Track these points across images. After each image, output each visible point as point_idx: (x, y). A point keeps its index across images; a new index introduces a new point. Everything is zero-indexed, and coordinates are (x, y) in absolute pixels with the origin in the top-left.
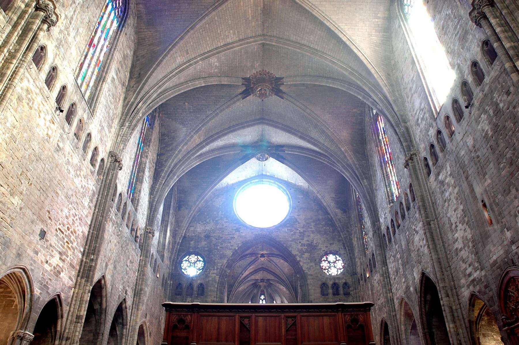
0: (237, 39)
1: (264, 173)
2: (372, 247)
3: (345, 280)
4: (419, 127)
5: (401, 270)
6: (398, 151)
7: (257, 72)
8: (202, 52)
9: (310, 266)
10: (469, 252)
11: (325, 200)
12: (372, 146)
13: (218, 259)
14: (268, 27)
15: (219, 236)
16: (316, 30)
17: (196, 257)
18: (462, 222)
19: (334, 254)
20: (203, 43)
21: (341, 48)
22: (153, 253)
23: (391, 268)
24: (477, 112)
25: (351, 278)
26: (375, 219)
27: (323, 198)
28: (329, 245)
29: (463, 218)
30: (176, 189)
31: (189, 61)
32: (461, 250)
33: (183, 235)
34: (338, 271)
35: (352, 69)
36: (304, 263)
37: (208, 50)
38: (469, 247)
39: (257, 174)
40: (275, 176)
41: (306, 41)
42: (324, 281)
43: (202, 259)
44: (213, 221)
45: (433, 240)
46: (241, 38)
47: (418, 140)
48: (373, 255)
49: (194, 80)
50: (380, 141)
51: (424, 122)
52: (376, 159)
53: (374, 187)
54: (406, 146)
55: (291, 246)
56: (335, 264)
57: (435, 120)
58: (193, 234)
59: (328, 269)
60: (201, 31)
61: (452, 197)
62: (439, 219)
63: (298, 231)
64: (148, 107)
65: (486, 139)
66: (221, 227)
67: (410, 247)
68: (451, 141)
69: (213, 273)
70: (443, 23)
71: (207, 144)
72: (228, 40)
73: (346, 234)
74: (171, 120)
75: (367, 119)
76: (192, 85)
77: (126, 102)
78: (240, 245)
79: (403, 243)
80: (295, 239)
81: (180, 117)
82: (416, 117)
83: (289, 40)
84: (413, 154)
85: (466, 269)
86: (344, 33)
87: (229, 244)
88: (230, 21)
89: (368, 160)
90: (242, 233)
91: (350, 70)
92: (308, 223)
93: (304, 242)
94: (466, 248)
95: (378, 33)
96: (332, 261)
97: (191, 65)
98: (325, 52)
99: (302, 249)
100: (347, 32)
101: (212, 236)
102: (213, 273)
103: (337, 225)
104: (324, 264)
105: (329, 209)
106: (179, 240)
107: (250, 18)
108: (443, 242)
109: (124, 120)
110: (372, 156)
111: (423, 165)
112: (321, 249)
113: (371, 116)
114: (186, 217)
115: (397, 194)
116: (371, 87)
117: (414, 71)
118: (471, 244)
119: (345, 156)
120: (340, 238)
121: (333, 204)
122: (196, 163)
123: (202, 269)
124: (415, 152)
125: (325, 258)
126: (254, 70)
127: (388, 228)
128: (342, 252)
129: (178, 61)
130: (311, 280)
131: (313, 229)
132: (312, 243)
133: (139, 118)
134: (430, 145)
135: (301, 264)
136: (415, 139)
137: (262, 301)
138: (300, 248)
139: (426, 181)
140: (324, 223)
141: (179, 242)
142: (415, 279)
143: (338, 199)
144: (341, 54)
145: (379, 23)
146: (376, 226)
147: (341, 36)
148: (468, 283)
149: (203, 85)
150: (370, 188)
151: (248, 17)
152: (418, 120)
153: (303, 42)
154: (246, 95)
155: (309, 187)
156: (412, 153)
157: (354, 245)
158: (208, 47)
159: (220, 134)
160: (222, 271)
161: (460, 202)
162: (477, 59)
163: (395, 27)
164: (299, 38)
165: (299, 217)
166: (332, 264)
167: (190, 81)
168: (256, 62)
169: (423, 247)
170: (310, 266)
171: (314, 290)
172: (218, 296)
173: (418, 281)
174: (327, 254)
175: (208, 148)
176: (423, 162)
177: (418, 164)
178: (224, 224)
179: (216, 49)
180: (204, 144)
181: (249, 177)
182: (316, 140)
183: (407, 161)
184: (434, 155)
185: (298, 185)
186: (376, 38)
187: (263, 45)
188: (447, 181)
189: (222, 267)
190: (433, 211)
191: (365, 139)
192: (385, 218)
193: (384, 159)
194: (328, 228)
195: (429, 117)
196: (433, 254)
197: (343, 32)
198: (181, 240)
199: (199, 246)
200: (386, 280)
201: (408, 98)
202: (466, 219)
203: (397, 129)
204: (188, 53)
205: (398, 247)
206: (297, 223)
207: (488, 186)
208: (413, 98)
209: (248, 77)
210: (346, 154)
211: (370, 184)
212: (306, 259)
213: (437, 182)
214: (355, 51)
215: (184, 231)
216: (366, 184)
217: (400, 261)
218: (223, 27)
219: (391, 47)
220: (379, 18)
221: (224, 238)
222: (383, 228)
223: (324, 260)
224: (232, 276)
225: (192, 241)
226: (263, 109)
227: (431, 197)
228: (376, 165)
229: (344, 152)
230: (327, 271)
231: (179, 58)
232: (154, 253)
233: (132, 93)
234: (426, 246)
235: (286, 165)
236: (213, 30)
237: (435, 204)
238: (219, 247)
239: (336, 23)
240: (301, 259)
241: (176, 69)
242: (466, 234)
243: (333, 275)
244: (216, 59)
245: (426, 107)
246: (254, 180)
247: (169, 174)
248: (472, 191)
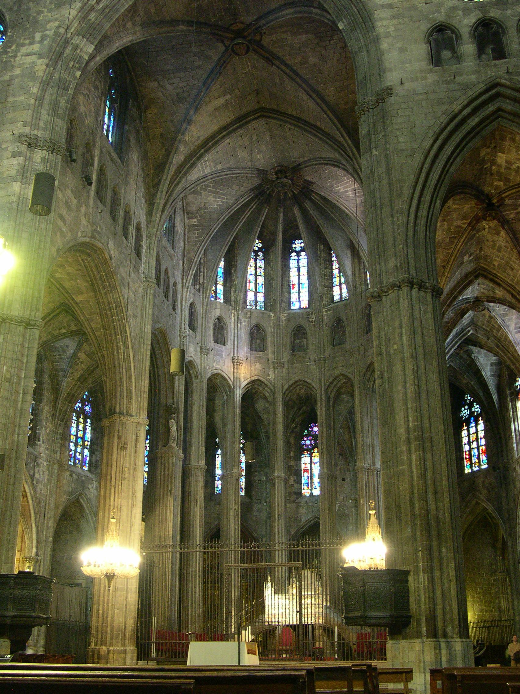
13: (49, 11)
42: (440, 17)
102: (27, 55)
130: (385, 23)
137: (298, 254)
171: (402, 50)
172: (42, 124)
189: (62, 30)
224: (162, 134)
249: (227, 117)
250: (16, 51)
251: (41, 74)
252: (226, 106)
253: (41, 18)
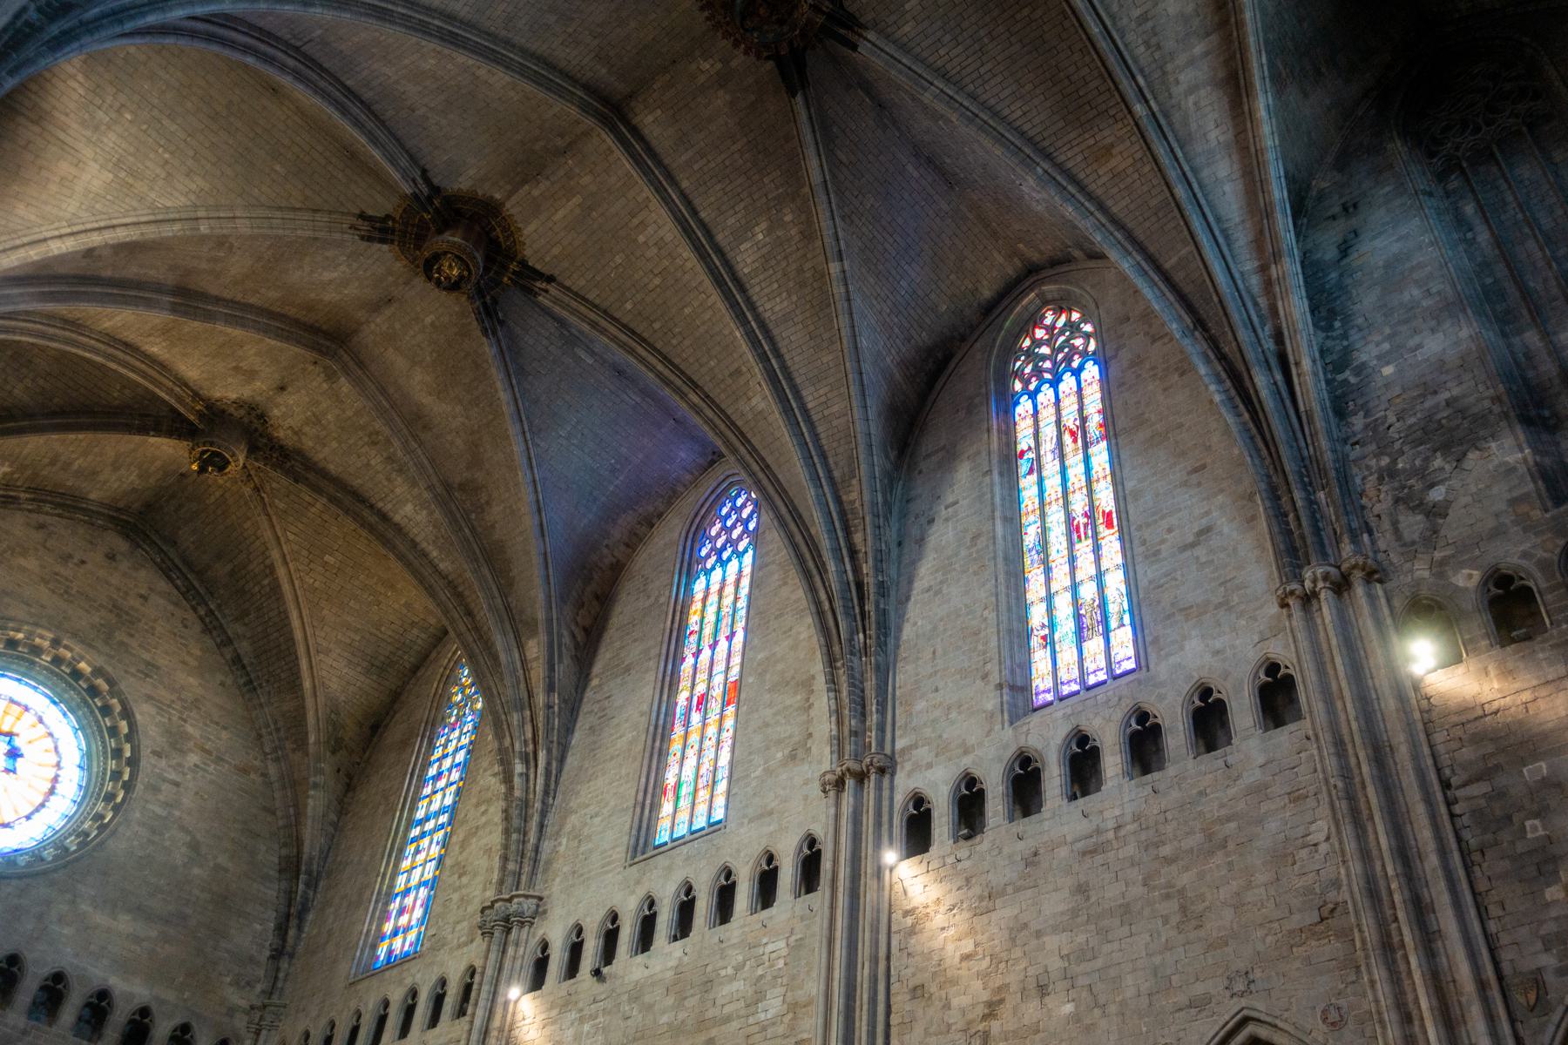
7: (736, 44)
14: (561, 135)
20: (703, 323)
60: (674, 342)
72: (669, 237)
88: (618, 260)
107: (577, 200)
129: (762, 405)
151: (578, 211)
168: (702, 79)
209: (770, 64)
236: (659, 301)
244: (743, 247)
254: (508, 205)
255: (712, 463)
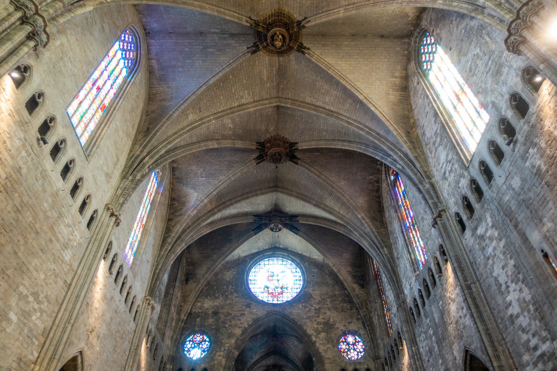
0: (252, 100)
1: (277, 246)
2: (397, 325)
3: (367, 365)
4: (447, 180)
5: (436, 349)
6: (422, 211)
7: (271, 137)
8: (215, 112)
9: (327, 348)
10: (529, 318)
11: (341, 274)
12: (390, 214)
13: (226, 339)
14: (283, 88)
15: (228, 313)
16: (332, 90)
17: (201, 337)
18: (516, 280)
19: (354, 333)
20: (217, 102)
21: (358, 107)
22: (151, 330)
23: (423, 348)
24: (523, 148)
25: (373, 363)
26: (399, 291)
27: (339, 272)
28: (347, 324)
29: (516, 276)
30: (184, 261)
31: (202, 119)
32: (518, 316)
33: (189, 311)
34: (358, 355)
35: (370, 129)
36: (320, 344)
37: (222, 109)
38: (529, 311)
39: (270, 247)
40: (289, 249)
41: (321, 103)
42: (343, 365)
43: (208, 340)
44: (222, 295)
45: (477, 307)
46: (256, 99)
47: (445, 195)
48: (399, 333)
49: (207, 140)
50: (399, 207)
51: (452, 175)
52: (396, 226)
53: (396, 255)
54: (432, 203)
55: (305, 324)
56: (355, 347)
57: (467, 169)
58: (200, 311)
59: (347, 352)
60: (215, 88)
61: (498, 253)
62: (481, 281)
63: (313, 308)
64: (156, 163)
65: (539, 176)
66: (230, 302)
67: (445, 320)
68: (490, 188)
69: (220, 356)
70: (471, 65)
71: (219, 211)
72: (242, 101)
73: (365, 312)
74: (182, 184)
75: (384, 185)
76: (204, 145)
77: (131, 155)
78: (250, 323)
79: (436, 316)
80: (310, 316)
81: (192, 182)
82: (443, 171)
83: (304, 102)
84: (442, 211)
85: (528, 341)
86: (360, 91)
87: (238, 322)
88: (244, 81)
89: (387, 228)
90: (253, 309)
91: (367, 129)
92: (324, 299)
93: (320, 320)
94: (526, 313)
95: (395, 93)
96: (351, 343)
97: (203, 123)
98: (341, 113)
99: (318, 328)
100: (364, 90)
101: (221, 313)
102: (220, 356)
103: (355, 302)
104: (343, 346)
105: (345, 284)
106: (183, 317)
107: (265, 79)
108: (490, 309)
109: (127, 173)
110: (391, 223)
111: (455, 222)
112: (338, 328)
113: (388, 183)
114: (194, 291)
115: (423, 260)
116: (390, 145)
117: (437, 124)
118: (531, 307)
119: (362, 224)
120: (359, 317)
121: (349, 279)
122: (206, 231)
123: (208, 350)
124: (444, 208)
125: (343, 339)
126: (268, 134)
127: (415, 300)
128: (362, 332)
130: (328, 365)
131: (330, 305)
132: (328, 321)
133: (145, 173)
134: (462, 198)
135: (317, 345)
136: (442, 195)
138: (316, 326)
139: (460, 239)
140: (341, 299)
141: (183, 320)
142: (455, 359)
143: (356, 274)
144: (358, 114)
145: (396, 82)
146: (401, 299)
147: (357, 94)
148: (535, 359)
149: (216, 146)
150: (392, 258)
151: (263, 77)
152: (445, 173)
153: (319, 104)
154: (259, 161)
155: (324, 260)
156: (440, 209)
157: (375, 324)
158: (221, 107)
159: (233, 201)
160: (230, 354)
161: (509, 256)
162: (517, 90)
163: (414, 85)
164: (314, 100)
165: (314, 292)
166: (351, 346)
167: (202, 141)
168: (270, 126)
169: (463, 318)
170: (327, 348)
173: (461, 361)
174: (345, 334)
175: (219, 216)
176: (454, 218)
177: (449, 220)
178: (234, 299)
179: (230, 109)
180: (216, 210)
181: (262, 249)
182: (330, 208)
183: (435, 219)
184: (469, 207)
185: (313, 259)
186: (394, 97)
187: (278, 107)
188: (488, 235)
190: (473, 272)
191: (383, 207)
192: (411, 289)
193: (405, 225)
194: (345, 305)
195: (459, 168)
196: (479, 324)
197: (359, 90)
198: (186, 316)
199: (205, 324)
200: (417, 363)
201: (431, 154)
202: (521, 276)
203: (420, 186)
204: (200, 111)
205: (430, 321)
206: (312, 299)
207: (548, 231)
208: (438, 152)
209: (263, 141)
210: (363, 222)
211: (391, 253)
212: (323, 340)
213: (475, 238)
214: (373, 109)
215: (190, 307)
216: (386, 252)
217: (434, 338)
218: (238, 87)
219: (409, 106)
220: (396, 77)
221: (233, 315)
222: (409, 300)
223: (342, 342)
225: (198, 318)
226: (277, 176)
227: (468, 257)
228: (397, 231)
229: (361, 219)
230: (346, 354)
231: (191, 115)
232: (153, 330)
233: (138, 146)
234: (468, 316)
235: (300, 236)
236: (228, 89)
237: (474, 263)
238: (227, 325)
239: (352, 82)
240: (317, 340)
241: (188, 126)
242: (523, 295)
243: (353, 358)
245: (454, 157)
246: (267, 252)
247: (177, 241)
248: (525, 240)
249: (263, 354)
250: (215, 354)
251: (224, 365)
252: (264, 351)
253: (223, 341)
254: (277, 58)
255: (145, 30)
